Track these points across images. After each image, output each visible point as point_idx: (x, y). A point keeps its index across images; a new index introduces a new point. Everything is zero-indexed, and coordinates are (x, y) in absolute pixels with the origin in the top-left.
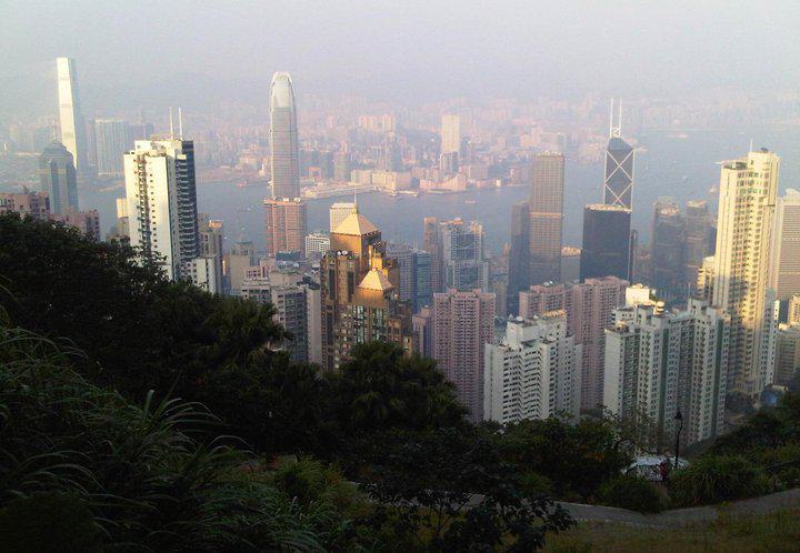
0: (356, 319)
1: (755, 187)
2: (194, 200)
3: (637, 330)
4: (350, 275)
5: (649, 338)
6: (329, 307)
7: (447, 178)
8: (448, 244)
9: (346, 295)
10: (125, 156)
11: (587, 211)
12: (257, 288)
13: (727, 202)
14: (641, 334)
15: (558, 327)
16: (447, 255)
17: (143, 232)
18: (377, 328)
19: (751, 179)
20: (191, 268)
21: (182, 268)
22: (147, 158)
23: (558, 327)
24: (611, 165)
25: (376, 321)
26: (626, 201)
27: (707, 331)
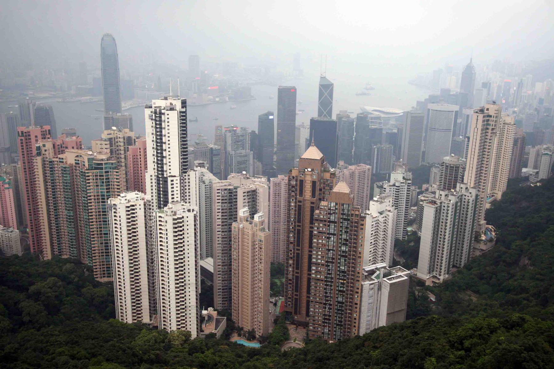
0: (330, 209)
1: (490, 122)
2: (187, 136)
3: (441, 203)
4: (314, 183)
5: (448, 207)
6: (300, 202)
7: (195, 95)
8: (229, 141)
9: (310, 194)
10: (146, 109)
11: (313, 121)
12: (226, 187)
13: (476, 131)
14: (443, 204)
15: (390, 201)
16: (229, 149)
17: (157, 156)
18: (343, 214)
19: (488, 118)
20: (187, 177)
21: (182, 178)
22: (163, 111)
23: (390, 201)
24: (321, 94)
25: (343, 210)
26: (330, 113)
27: (471, 201)
